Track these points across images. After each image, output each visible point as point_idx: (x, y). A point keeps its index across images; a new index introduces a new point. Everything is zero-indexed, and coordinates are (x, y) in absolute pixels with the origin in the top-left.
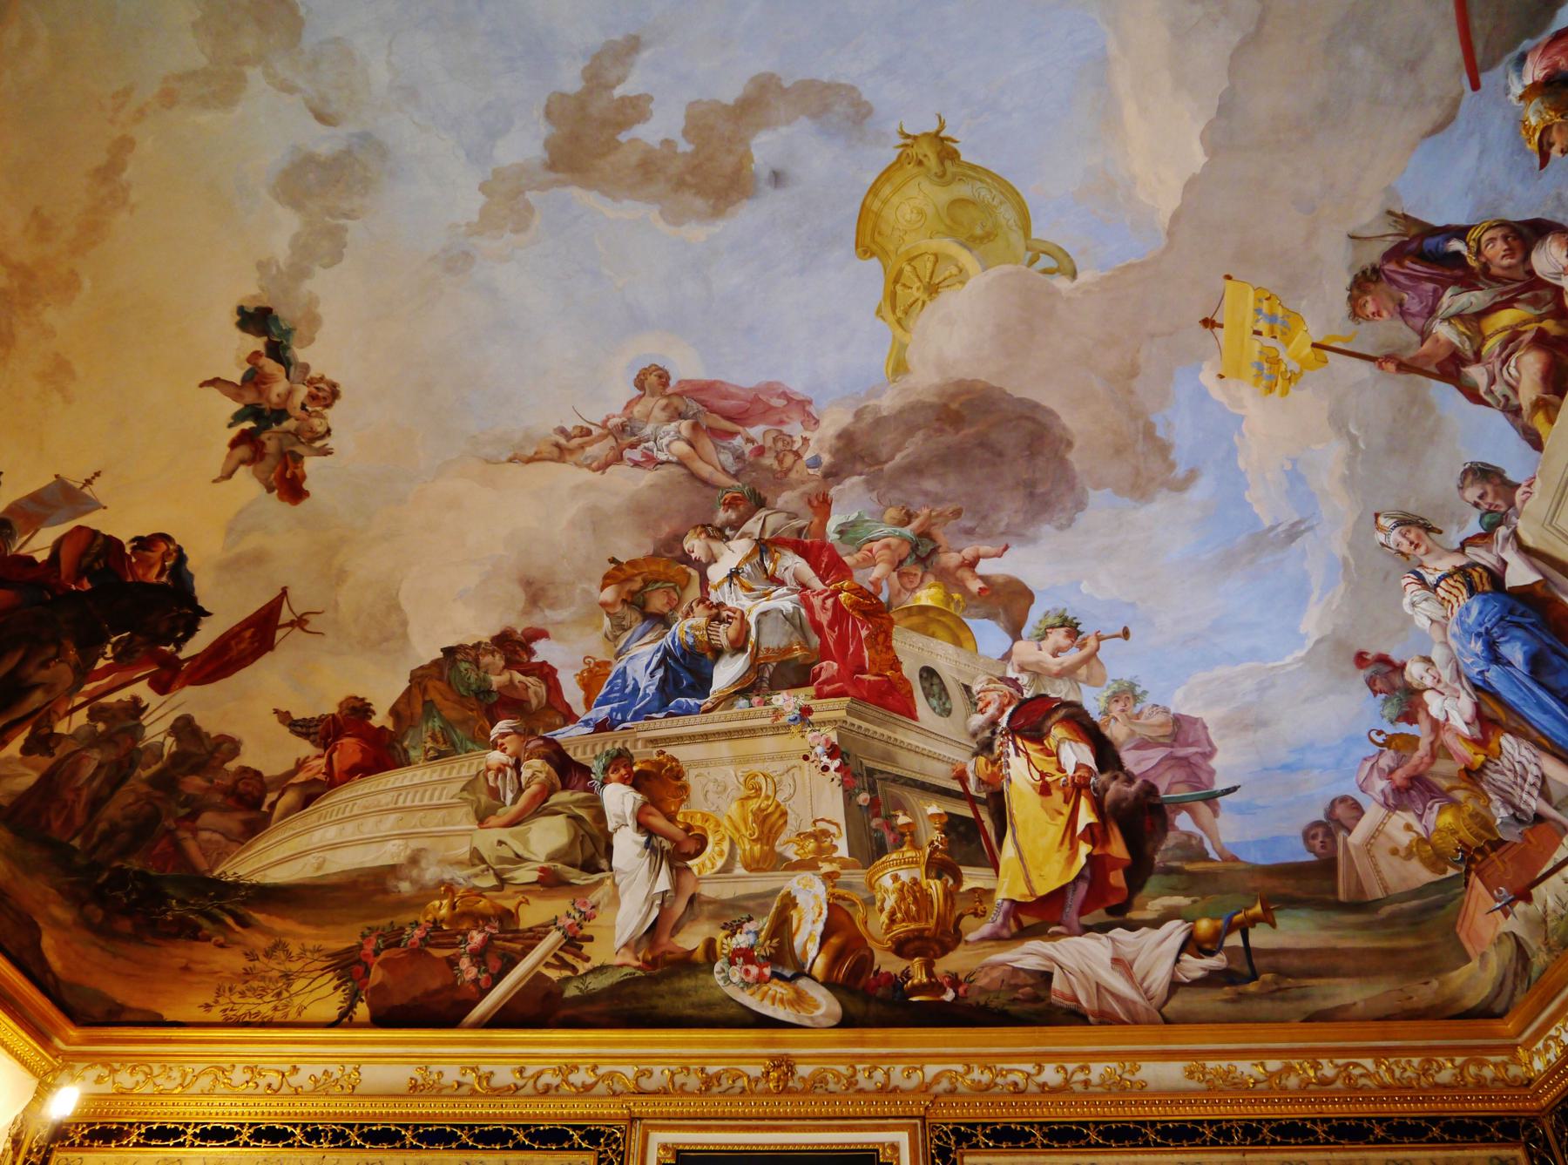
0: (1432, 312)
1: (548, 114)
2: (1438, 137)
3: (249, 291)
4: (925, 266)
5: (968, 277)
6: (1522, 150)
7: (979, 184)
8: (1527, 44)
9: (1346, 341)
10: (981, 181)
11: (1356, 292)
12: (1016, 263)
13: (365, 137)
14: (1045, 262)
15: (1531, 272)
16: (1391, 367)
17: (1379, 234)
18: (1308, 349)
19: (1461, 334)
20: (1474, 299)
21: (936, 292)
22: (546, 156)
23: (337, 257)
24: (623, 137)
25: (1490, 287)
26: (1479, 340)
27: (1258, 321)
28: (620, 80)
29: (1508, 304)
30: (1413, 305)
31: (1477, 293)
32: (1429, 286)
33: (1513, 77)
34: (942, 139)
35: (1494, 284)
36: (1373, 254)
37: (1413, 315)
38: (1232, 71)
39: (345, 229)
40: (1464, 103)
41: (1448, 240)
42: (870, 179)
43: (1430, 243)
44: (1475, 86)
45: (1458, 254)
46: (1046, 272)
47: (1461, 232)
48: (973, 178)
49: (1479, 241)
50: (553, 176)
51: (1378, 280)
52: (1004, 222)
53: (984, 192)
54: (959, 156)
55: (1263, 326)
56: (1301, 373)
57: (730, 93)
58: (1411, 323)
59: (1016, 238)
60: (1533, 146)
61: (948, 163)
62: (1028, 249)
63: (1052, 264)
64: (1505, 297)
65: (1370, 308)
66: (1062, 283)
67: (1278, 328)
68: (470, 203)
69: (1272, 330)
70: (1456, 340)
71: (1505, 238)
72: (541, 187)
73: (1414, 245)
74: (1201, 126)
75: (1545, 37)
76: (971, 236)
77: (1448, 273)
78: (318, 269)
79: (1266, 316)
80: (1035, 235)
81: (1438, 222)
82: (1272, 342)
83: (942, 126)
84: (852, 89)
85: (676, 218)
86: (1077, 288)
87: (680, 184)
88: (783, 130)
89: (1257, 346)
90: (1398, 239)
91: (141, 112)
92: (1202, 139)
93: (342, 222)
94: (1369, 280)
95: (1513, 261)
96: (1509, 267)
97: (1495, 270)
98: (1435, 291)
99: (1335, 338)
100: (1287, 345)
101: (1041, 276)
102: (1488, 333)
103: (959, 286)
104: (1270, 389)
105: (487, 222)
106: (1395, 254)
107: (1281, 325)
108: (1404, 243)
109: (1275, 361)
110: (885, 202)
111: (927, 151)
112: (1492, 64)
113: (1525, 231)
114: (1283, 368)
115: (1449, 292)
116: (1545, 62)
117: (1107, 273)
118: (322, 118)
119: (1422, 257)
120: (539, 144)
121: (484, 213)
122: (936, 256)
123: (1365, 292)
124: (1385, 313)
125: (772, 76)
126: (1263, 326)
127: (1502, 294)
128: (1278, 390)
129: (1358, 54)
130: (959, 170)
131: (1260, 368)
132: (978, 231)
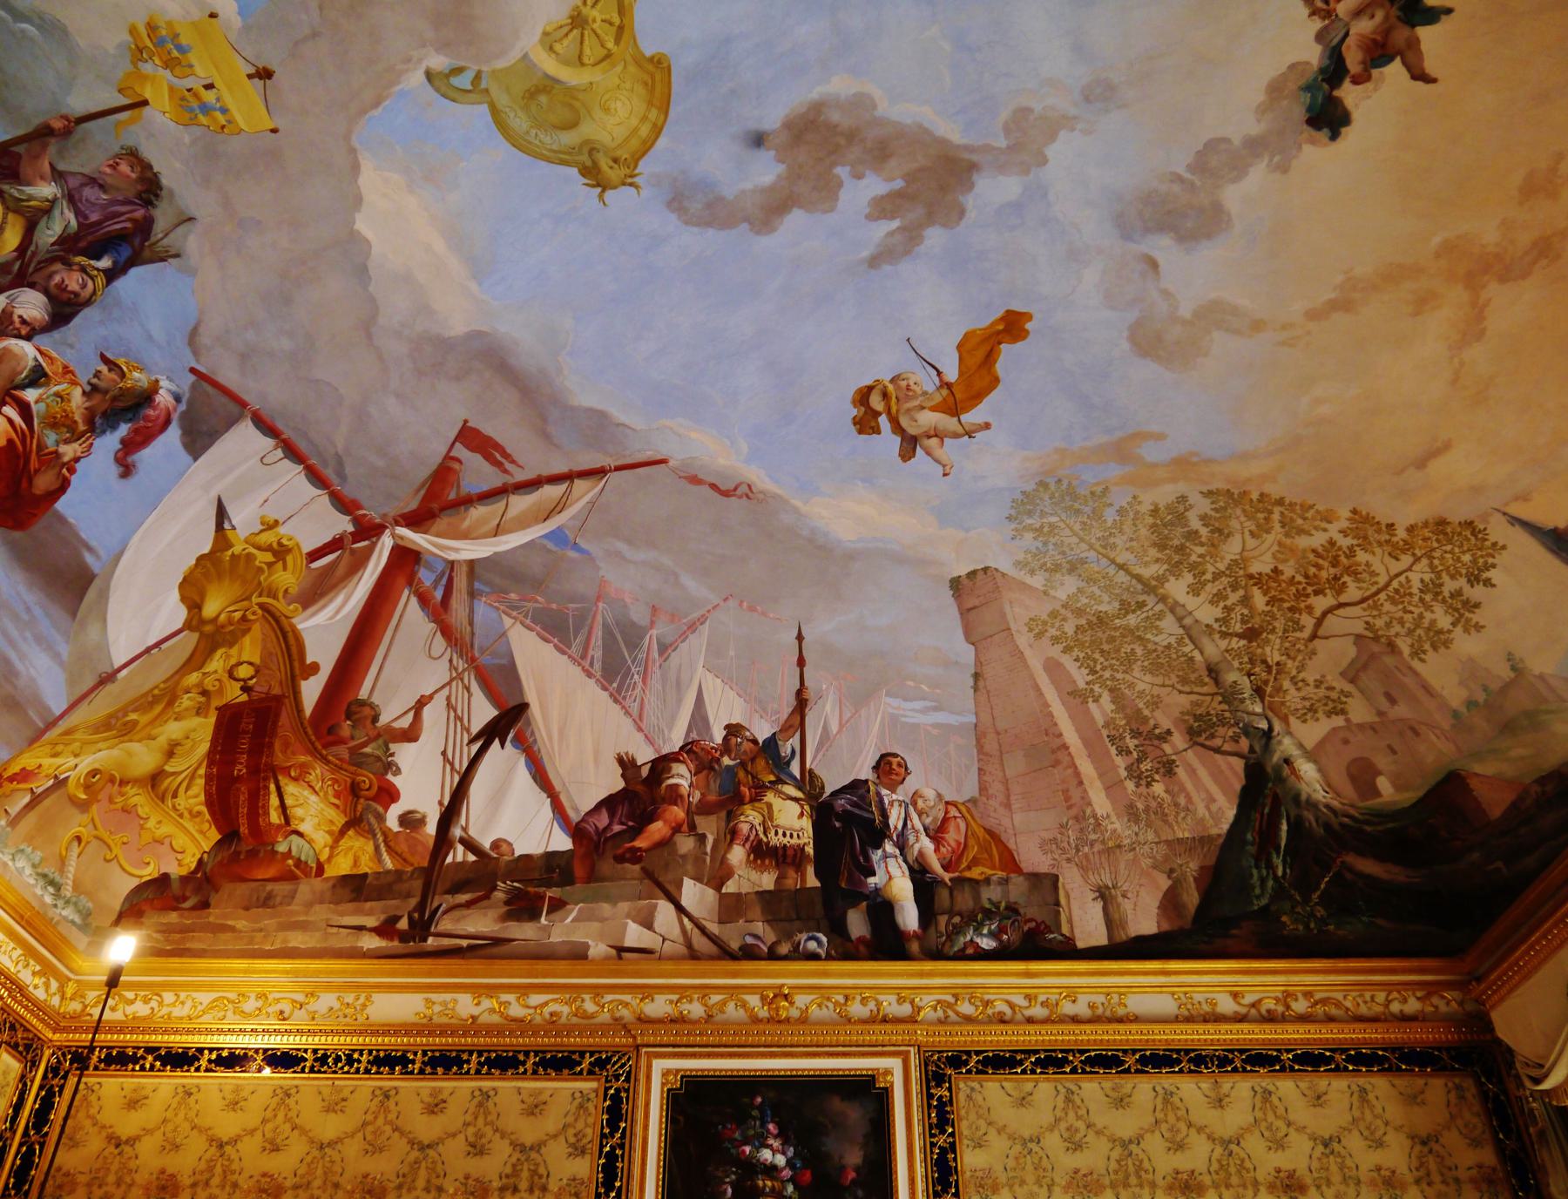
0: (72, 199)
1: (962, 213)
2: (190, 328)
3: (1317, 154)
4: (591, 51)
5: (542, 42)
6: (126, 355)
7: (554, 147)
8: (183, 407)
9: (118, 124)
10: (551, 151)
11: (149, 175)
12: (493, 71)
13: (1127, 235)
14: (464, 81)
15: (32, 286)
16: (57, 124)
17: (172, 236)
18: (148, 95)
19: (30, 198)
20: (49, 233)
21: (572, 17)
22: (975, 177)
23: (1212, 145)
24: (899, 184)
25: (48, 252)
26: (11, 204)
27: (218, 100)
28: (891, 234)
29: (22, 249)
30: (88, 193)
31: (53, 240)
32: (94, 217)
33: (173, 388)
34: (598, 185)
35: (48, 256)
36: (162, 217)
37: (83, 185)
38: (372, 300)
39: (1189, 168)
40: (188, 352)
41: (115, 263)
42: (662, 142)
43: (126, 252)
44: (193, 371)
45: (98, 258)
46: (458, 71)
47: (111, 275)
48: (560, 152)
49: (92, 278)
50: (975, 158)
51: (139, 196)
52: (520, 113)
53: (548, 140)
54: (580, 171)
55: (209, 97)
56: (134, 64)
57: (796, 219)
58: (80, 177)
59: (502, 100)
60: (121, 362)
61: (589, 163)
62: (487, 91)
63: (456, 81)
64: (29, 253)
65: (124, 168)
66: (439, 62)
67: (194, 104)
68: (1061, 151)
69: (196, 96)
70: (29, 190)
71: (76, 294)
72: (987, 149)
73: (137, 241)
74: (376, 250)
75: (175, 417)
76: (549, 92)
77: (90, 238)
78: (1237, 141)
79: (215, 109)
80: (484, 108)
81: (135, 272)
82: (188, 82)
83: (601, 196)
84: (686, 223)
85: (861, 102)
86: (420, 61)
87: (852, 136)
88: (748, 186)
89: (199, 70)
90: (153, 239)
91: (1284, 327)
92: (367, 241)
93: (1187, 176)
94: (148, 191)
95: (53, 283)
96: (50, 276)
97: (58, 266)
98: (86, 217)
99: (132, 121)
100: (171, 89)
101: (462, 64)
102: (11, 216)
103: (549, 29)
104: (152, 27)
105: (1053, 127)
106: (145, 226)
107: (191, 107)
108: (147, 239)
109: (170, 64)
110: (644, 119)
111: (613, 174)
112: (193, 387)
113: (68, 310)
114: (157, 61)
115: (74, 223)
116: (162, 406)
117: (397, 88)
118: (1154, 264)
119: (121, 238)
120: (976, 190)
121: (1052, 137)
122: (583, 64)
123: (141, 179)
124: (108, 170)
125: (758, 233)
126: (209, 97)
127: (34, 254)
128: (143, 31)
129: (286, 344)
130: (576, 158)
131: (179, 48)
132: (543, 99)
